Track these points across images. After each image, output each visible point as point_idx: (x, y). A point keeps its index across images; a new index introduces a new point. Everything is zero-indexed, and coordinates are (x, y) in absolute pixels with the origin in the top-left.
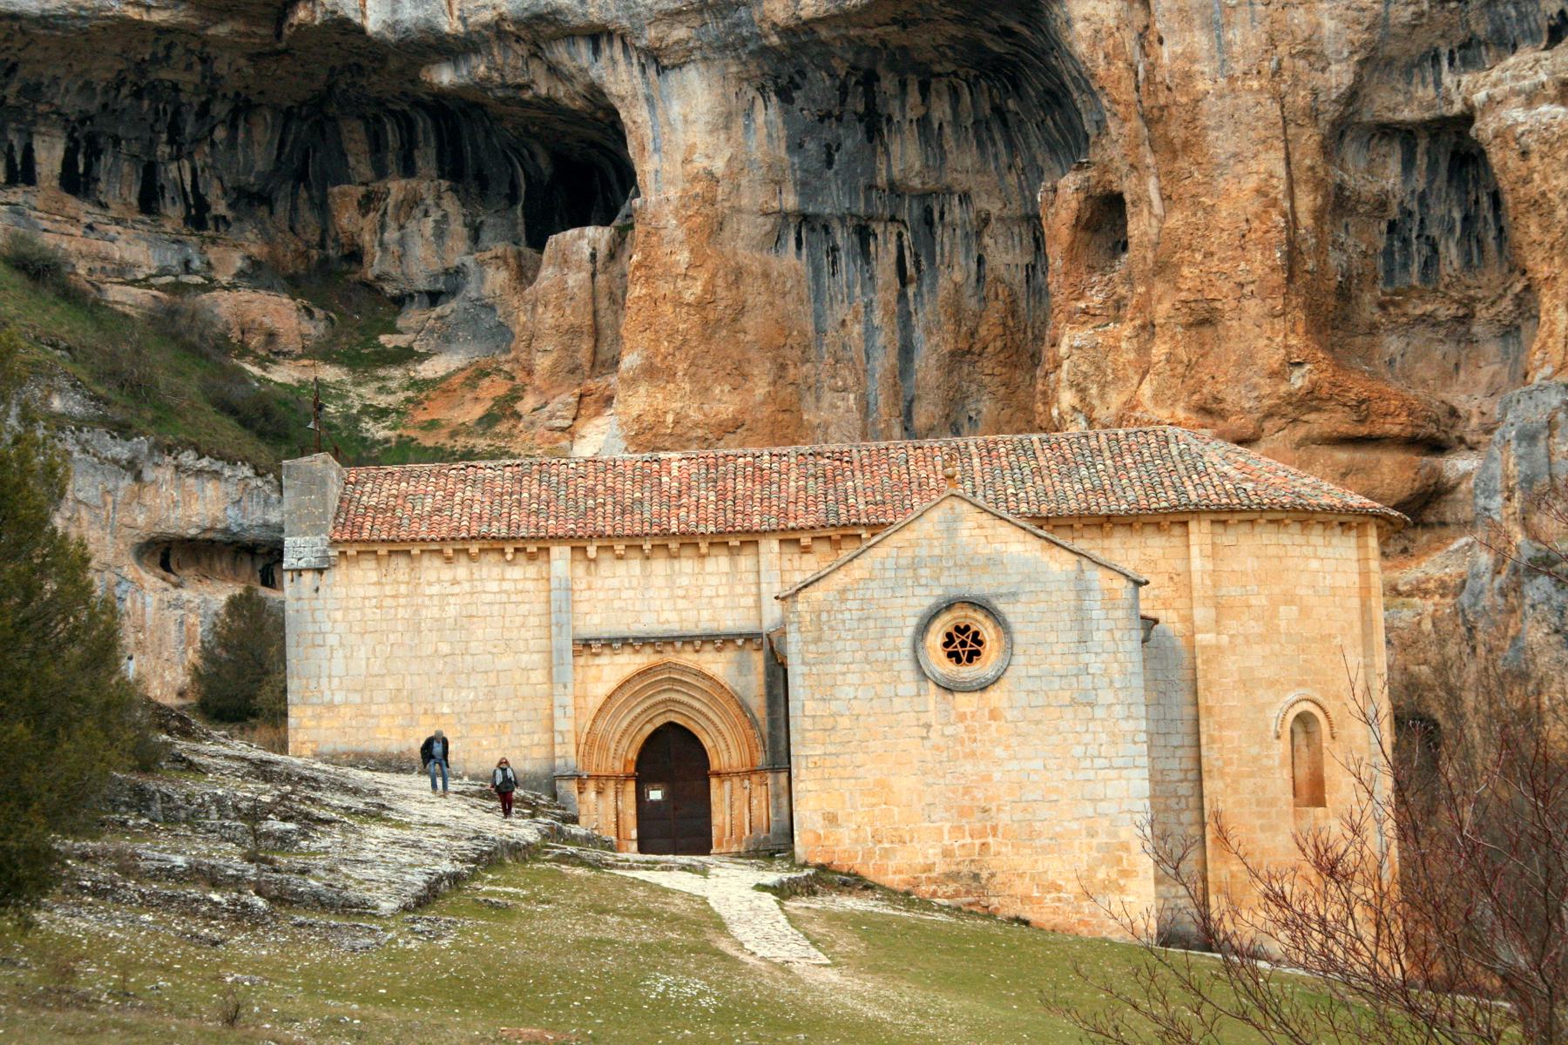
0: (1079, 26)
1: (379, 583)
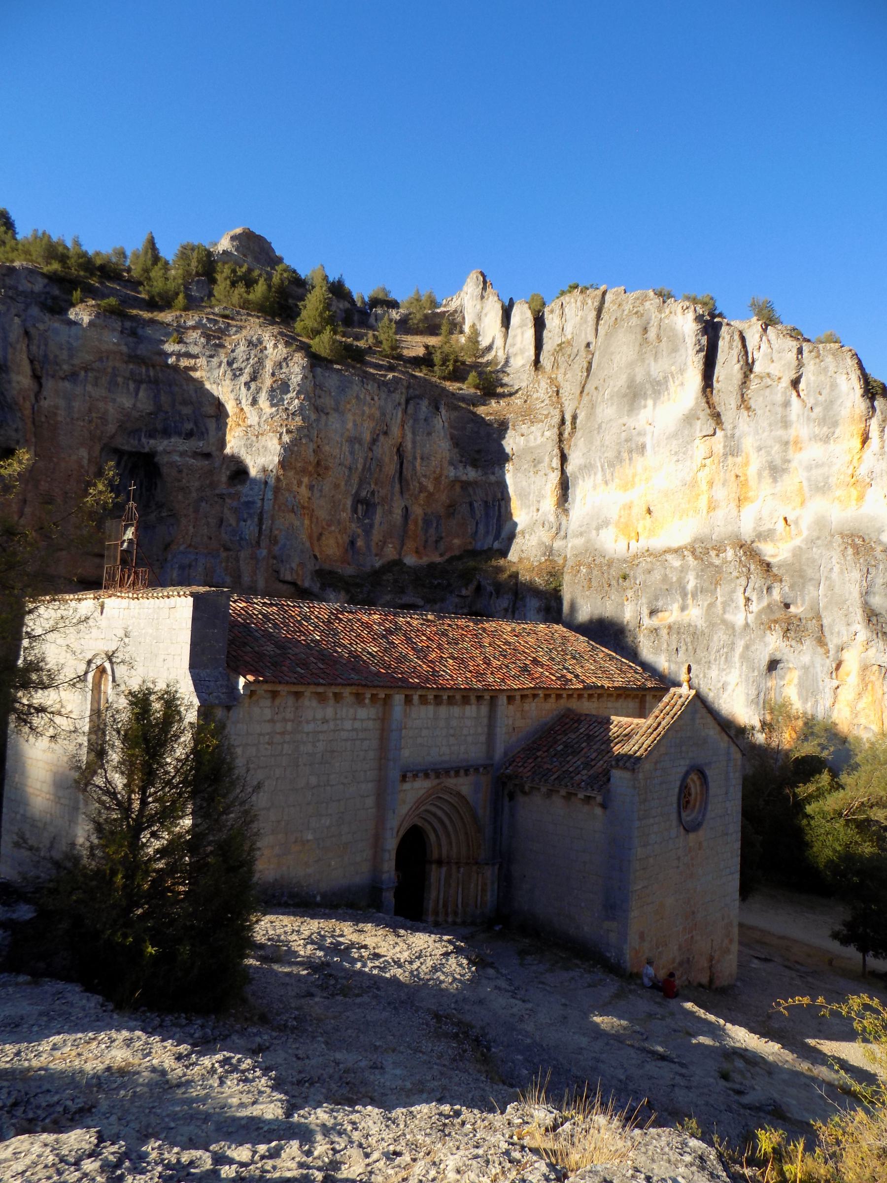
0: (14, 384)
1: (272, 721)
